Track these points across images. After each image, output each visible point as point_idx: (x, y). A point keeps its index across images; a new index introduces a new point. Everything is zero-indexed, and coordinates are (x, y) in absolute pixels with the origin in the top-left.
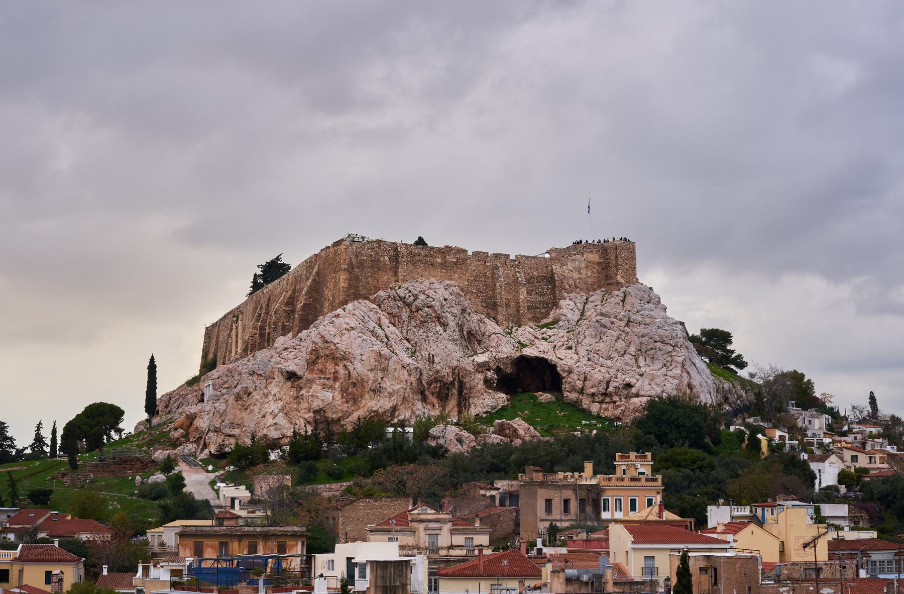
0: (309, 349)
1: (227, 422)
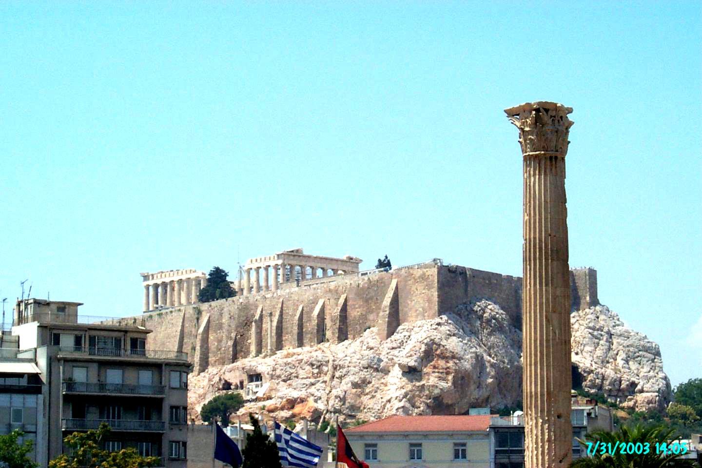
0: (423, 349)
1: (347, 405)
